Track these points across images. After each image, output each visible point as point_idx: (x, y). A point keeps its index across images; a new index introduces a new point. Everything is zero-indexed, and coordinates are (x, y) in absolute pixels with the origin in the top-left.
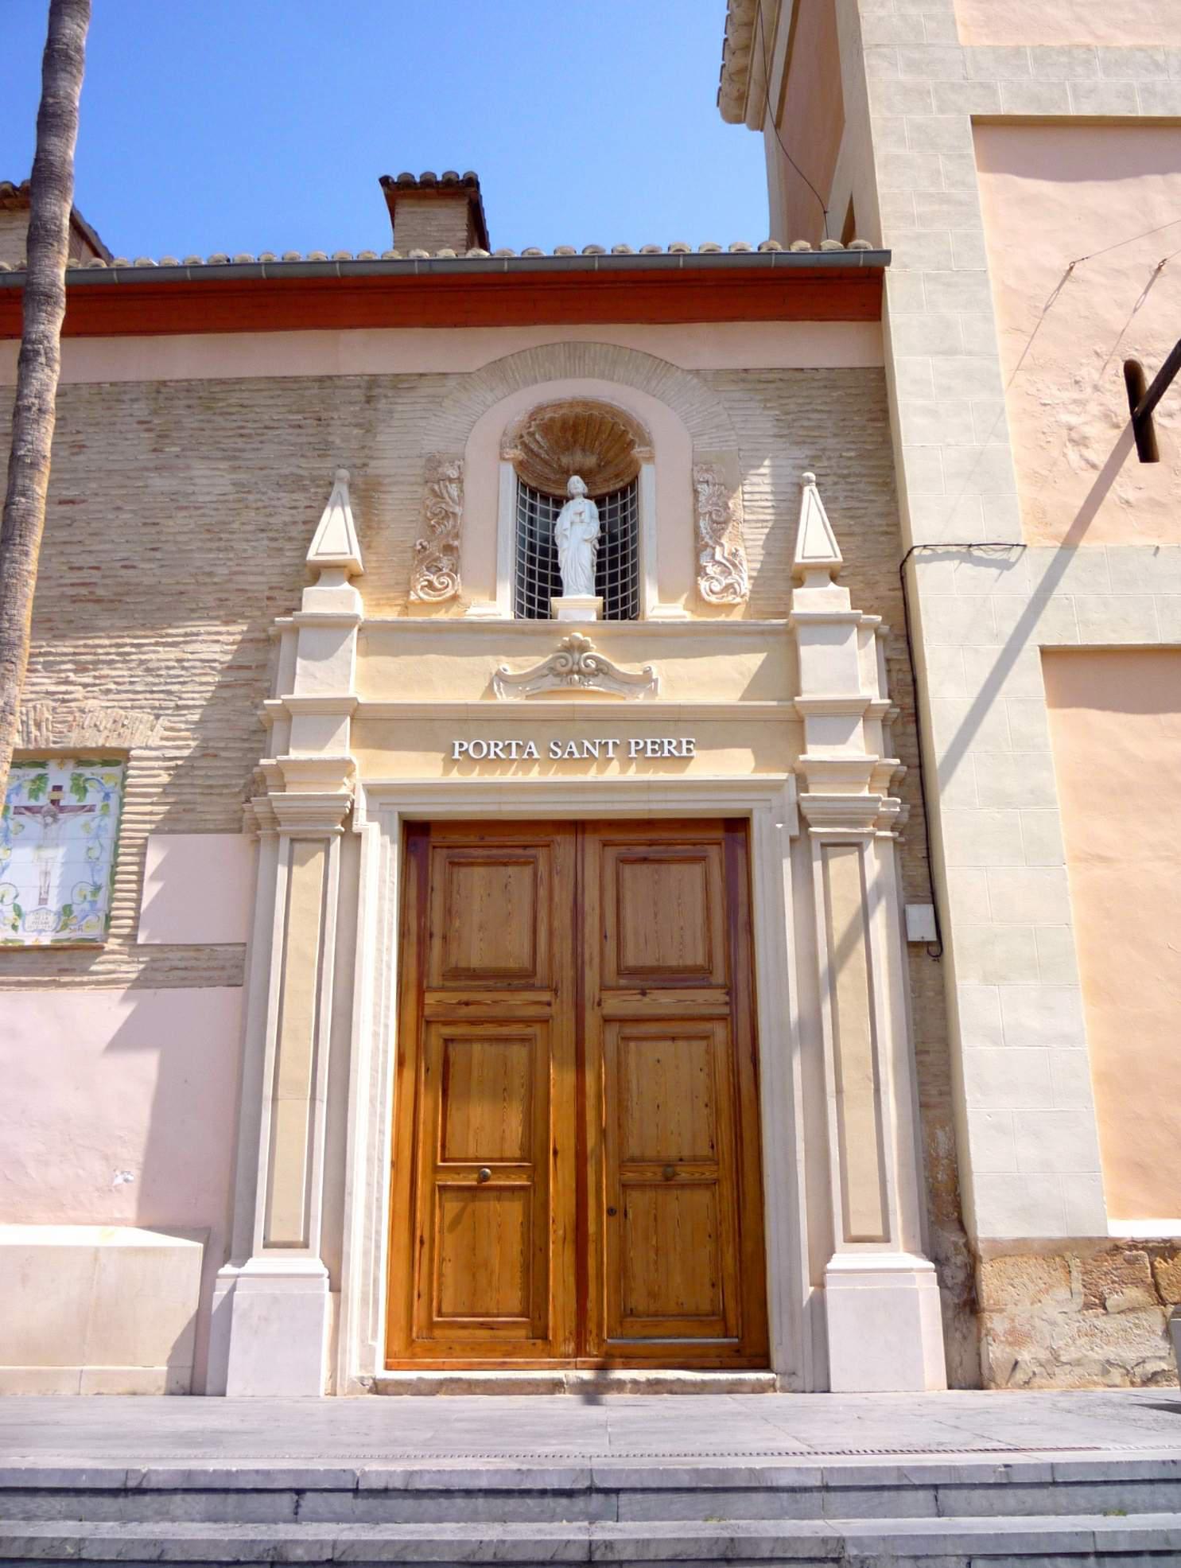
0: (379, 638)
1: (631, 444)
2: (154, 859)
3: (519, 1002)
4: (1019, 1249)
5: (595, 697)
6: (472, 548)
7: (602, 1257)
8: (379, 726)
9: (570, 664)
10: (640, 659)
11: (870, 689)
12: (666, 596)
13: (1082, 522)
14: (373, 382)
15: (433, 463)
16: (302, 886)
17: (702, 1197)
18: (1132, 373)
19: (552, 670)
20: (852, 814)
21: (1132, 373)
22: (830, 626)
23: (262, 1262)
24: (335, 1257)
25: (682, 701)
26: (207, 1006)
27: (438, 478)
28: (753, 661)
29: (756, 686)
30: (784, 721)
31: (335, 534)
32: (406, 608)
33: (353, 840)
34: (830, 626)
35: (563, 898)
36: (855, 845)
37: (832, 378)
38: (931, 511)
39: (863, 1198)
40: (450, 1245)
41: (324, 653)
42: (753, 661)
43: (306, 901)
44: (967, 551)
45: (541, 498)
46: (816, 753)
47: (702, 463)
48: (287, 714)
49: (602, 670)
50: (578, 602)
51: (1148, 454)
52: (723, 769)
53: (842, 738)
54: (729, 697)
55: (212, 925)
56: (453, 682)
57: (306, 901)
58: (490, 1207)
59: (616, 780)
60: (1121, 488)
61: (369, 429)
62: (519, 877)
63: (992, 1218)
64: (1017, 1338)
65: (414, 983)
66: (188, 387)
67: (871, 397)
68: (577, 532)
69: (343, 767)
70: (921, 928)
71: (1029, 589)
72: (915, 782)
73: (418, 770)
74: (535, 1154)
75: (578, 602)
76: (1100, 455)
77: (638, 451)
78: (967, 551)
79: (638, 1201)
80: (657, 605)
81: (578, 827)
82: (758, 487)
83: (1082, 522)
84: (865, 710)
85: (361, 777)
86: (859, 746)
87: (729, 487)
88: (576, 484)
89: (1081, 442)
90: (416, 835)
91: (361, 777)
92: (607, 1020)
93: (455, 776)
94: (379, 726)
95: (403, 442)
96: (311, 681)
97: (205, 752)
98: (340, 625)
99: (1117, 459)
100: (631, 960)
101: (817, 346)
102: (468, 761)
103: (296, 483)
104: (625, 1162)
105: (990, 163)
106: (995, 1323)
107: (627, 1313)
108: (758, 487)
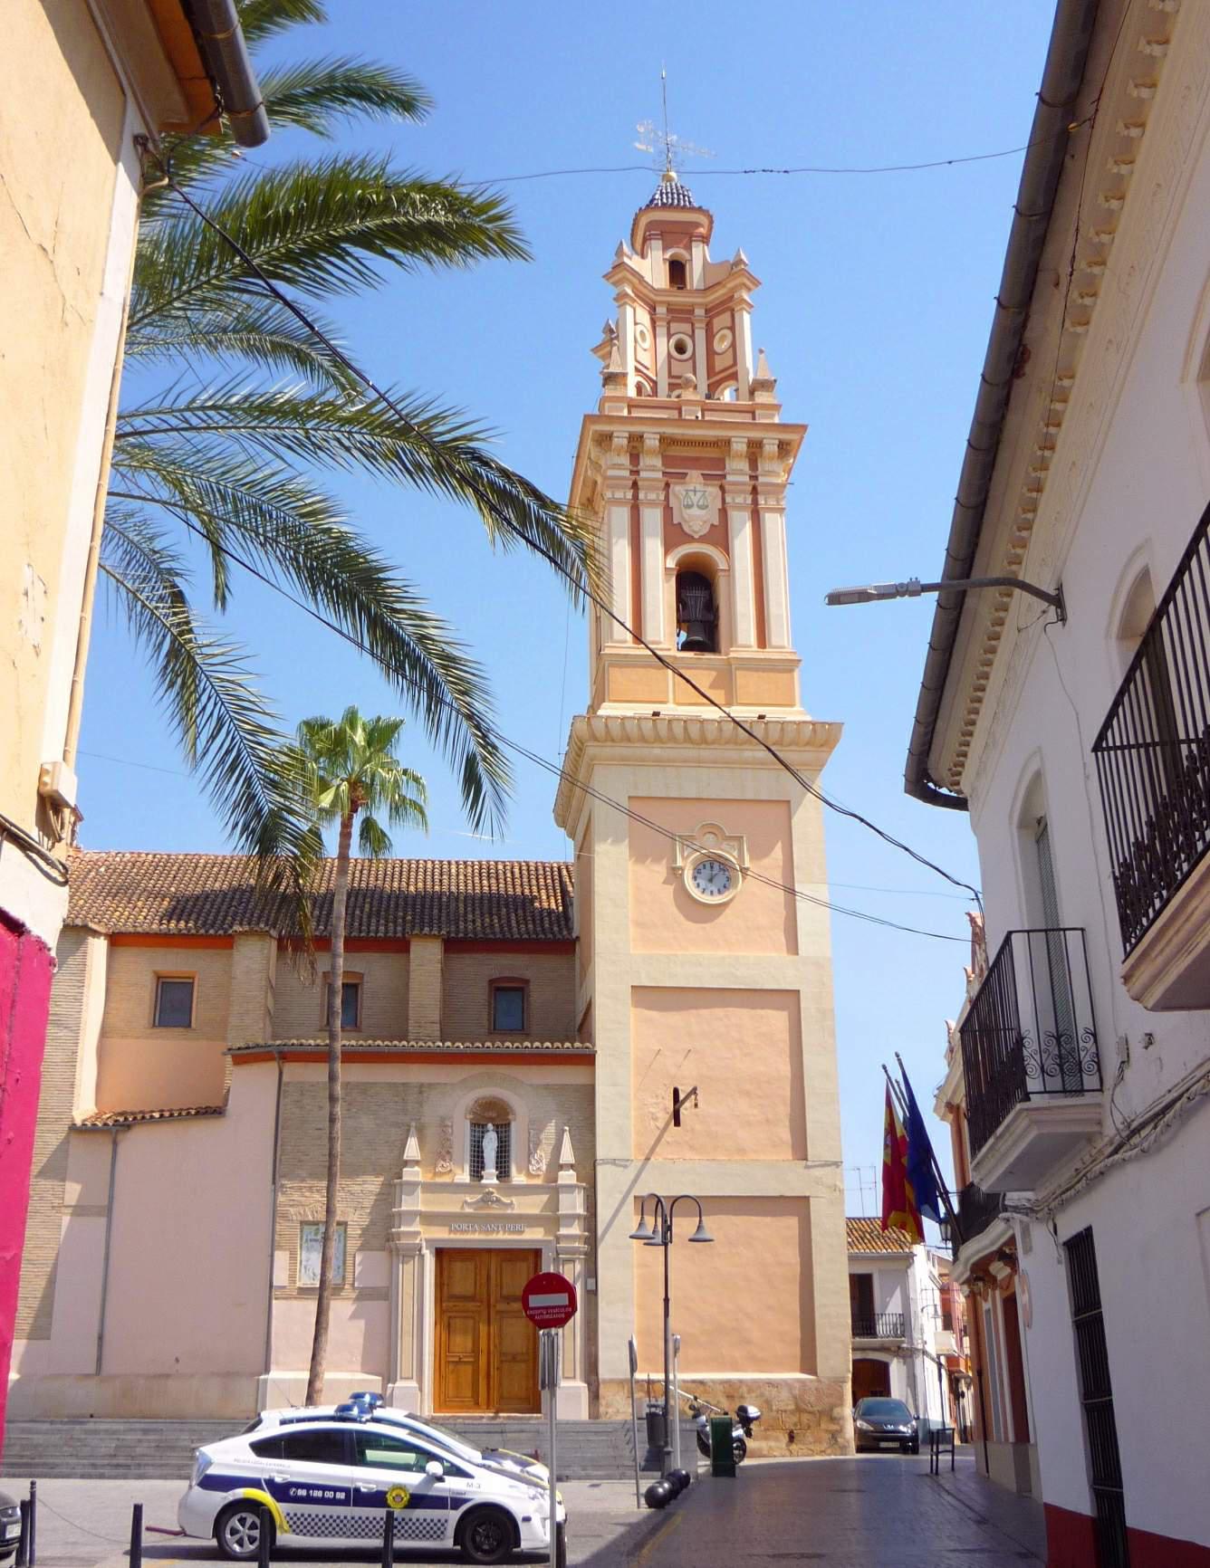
0: (429, 1188)
2: (358, 1259)
3: (471, 1305)
4: (611, 1381)
5: (495, 1210)
6: (456, 1151)
7: (494, 1383)
8: (430, 1219)
9: (487, 1199)
10: (509, 1195)
11: (581, 1210)
12: (519, 1171)
13: (652, 1150)
14: (422, 1085)
15: (443, 1119)
16: (406, 1271)
17: (523, 1366)
18: (676, 1092)
19: (482, 1200)
20: (574, 1251)
21: (676, 1092)
22: (570, 1188)
23: (399, 1384)
24: (420, 1381)
25: (522, 1211)
26: (379, 1306)
27: (444, 1125)
28: (545, 1198)
29: (545, 1208)
30: (552, 1220)
31: (412, 1149)
32: (435, 1174)
33: (422, 1257)
34: (570, 1188)
35: (484, 1273)
36: (573, 1261)
37: (577, 1088)
38: (605, 1146)
39: (569, 1366)
40: (451, 1377)
41: (411, 1193)
42: (545, 1198)
43: (408, 1277)
44: (614, 1162)
45: (478, 1128)
46: (563, 1231)
47: (532, 1122)
48: (400, 1214)
49: (498, 1200)
50: (490, 1177)
51: (677, 1123)
52: (533, 1235)
53: (570, 1225)
54: (536, 1211)
55: (379, 1281)
56: (450, 1204)
57: (408, 1277)
58: (462, 1368)
59: (502, 1237)
60: (667, 1137)
61: (421, 1104)
62: (470, 1266)
63: (604, 1373)
64: (608, 1406)
65: (439, 1300)
66: (358, 1085)
67: (588, 1095)
69: (418, 1233)
70: (591, 1286)
71: (632, 1177)
72: (592, 1240)
73: (442, 1234)
74: (476, 1351)
75: (490, 1177)
76: (661, 1124)
78: (614, 1162)
79: (506, 1366)
80: (518, 1178)
81: (489, 1251)
82: (551, 1129)
83: (652, 1150)
84: (578, 1216)
85: (423, 1236)
86: (576, 1229)
87: (541, 1130)
88: (490, 1126)
89: (656, 1119)
90: (440, 1254)
91: (423, 1236)
93: (452, 1236)
94: (430, 1219)
95: (434, 1108)
96: (408, 1204)
97: (372, 1223)
98: (415, 1185)
99: (667, 1125)
100: (505, 1292)
101: (569, 1076)
102: (456, 1231)
103: (397, 1125)
104: (502, 1354)
105: (638, 1003)
106: (602, 1402)
107: (501, 1397)
108: (551, 1129)
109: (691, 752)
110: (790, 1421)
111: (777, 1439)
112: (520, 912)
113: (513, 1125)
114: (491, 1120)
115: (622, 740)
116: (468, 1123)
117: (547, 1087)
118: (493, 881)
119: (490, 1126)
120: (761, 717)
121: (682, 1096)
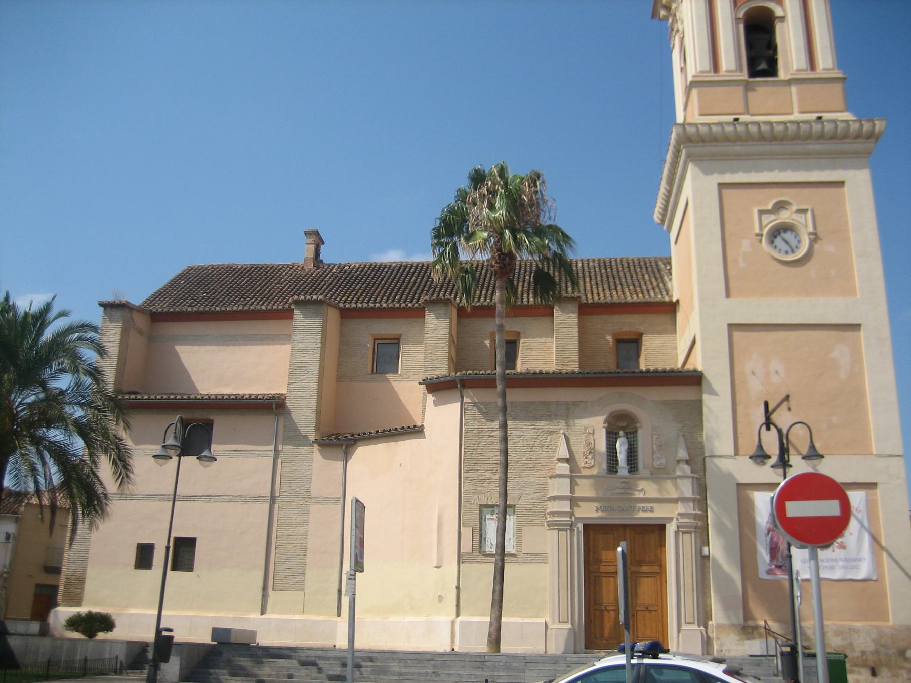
1: (635, 423)
14: (567, 403)
18: (766, 404)
21: (766, 404)
68: (621, 447)
77: (638, 425)
88: (621, 433)
92: (632, 573)
109: (766, 148)
110: (872, 659)
111: (860, 673)
112: (631, 287)
113: (640, 432)
114: (623, 428)
115: (711, 141)
116: (604, 430)
117: (664, 403)
118: (609, 270)
119: (621, 433)
120: (820, 118)
121: (771, 408)
